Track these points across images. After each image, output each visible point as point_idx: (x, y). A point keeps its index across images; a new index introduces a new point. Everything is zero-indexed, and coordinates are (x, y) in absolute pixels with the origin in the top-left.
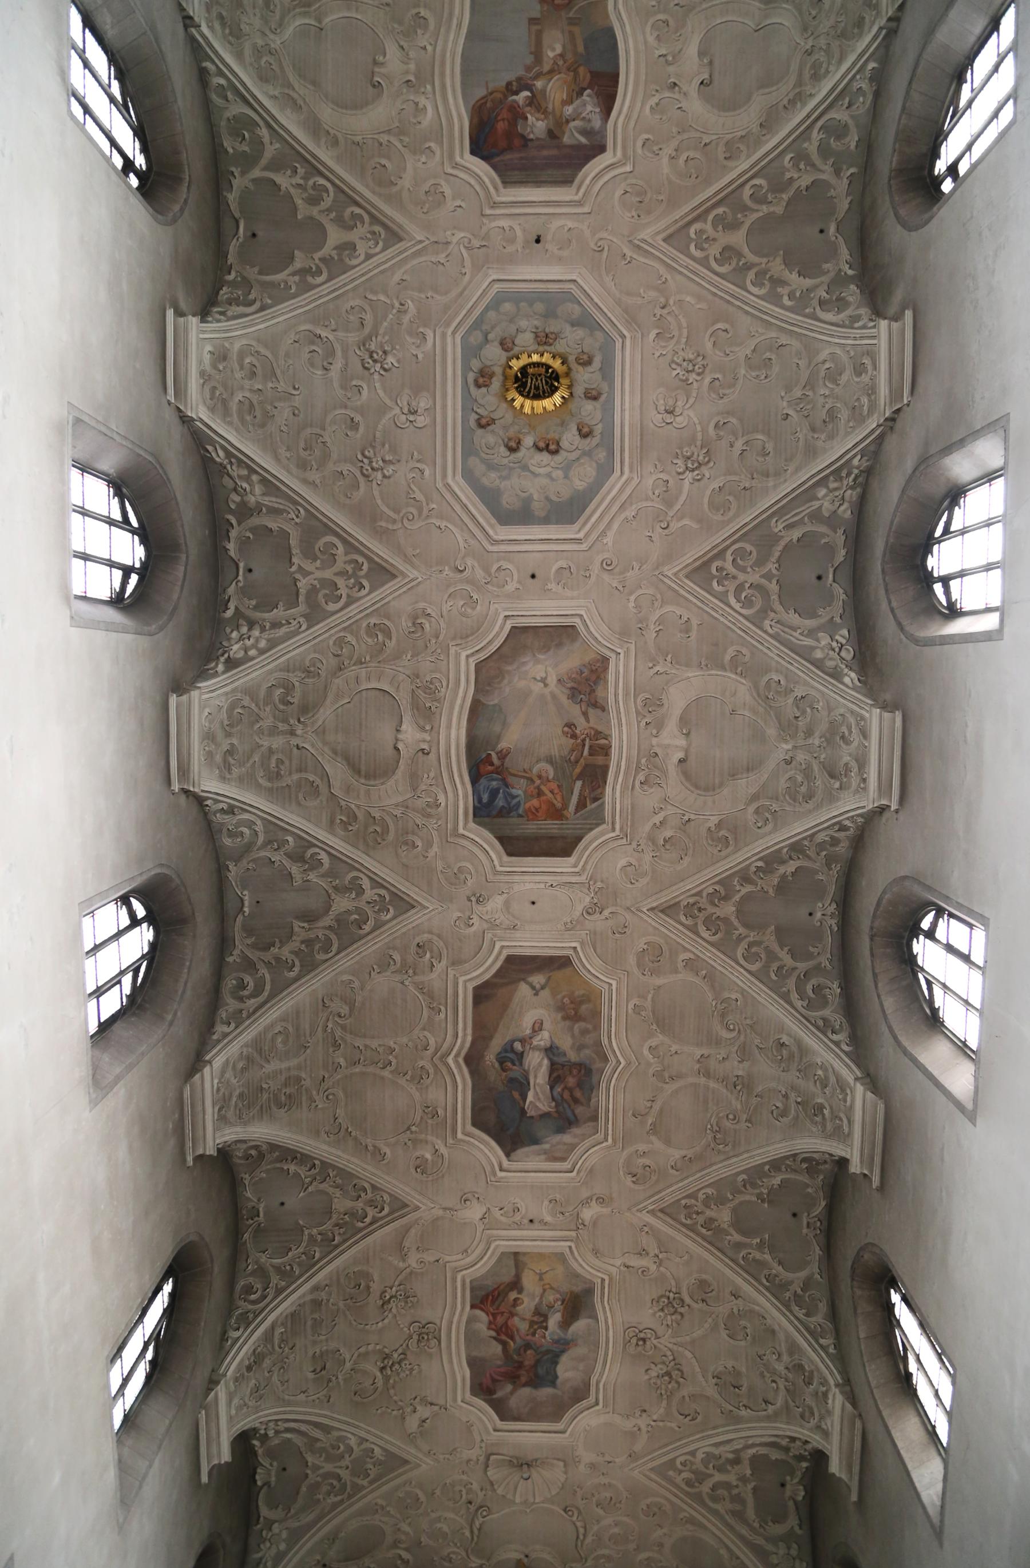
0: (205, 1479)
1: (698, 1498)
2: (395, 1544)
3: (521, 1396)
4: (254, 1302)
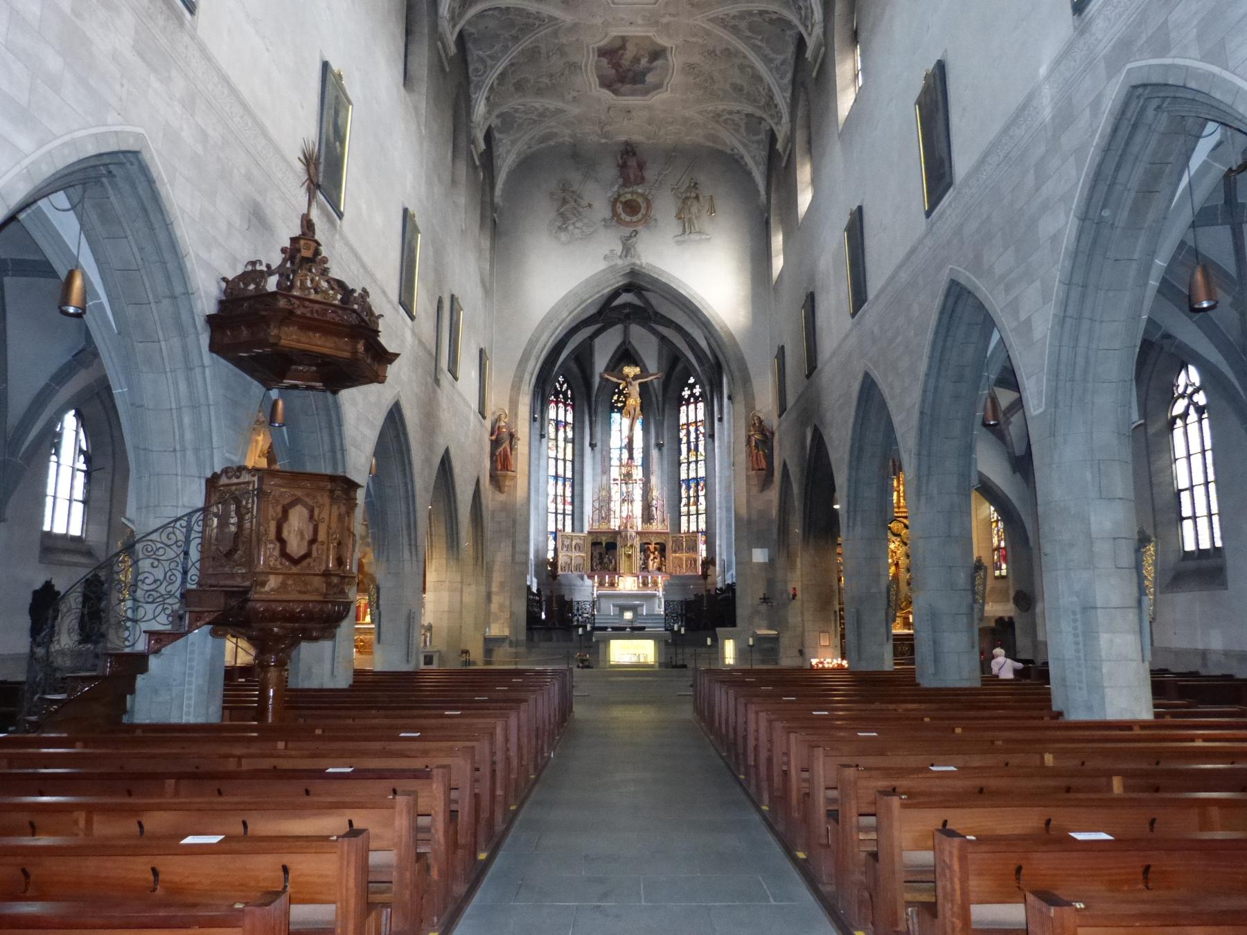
0: (478, 163)
1: (717, 122)
2: (563, 137)
3: (627, 87)
4: (480, 76)
